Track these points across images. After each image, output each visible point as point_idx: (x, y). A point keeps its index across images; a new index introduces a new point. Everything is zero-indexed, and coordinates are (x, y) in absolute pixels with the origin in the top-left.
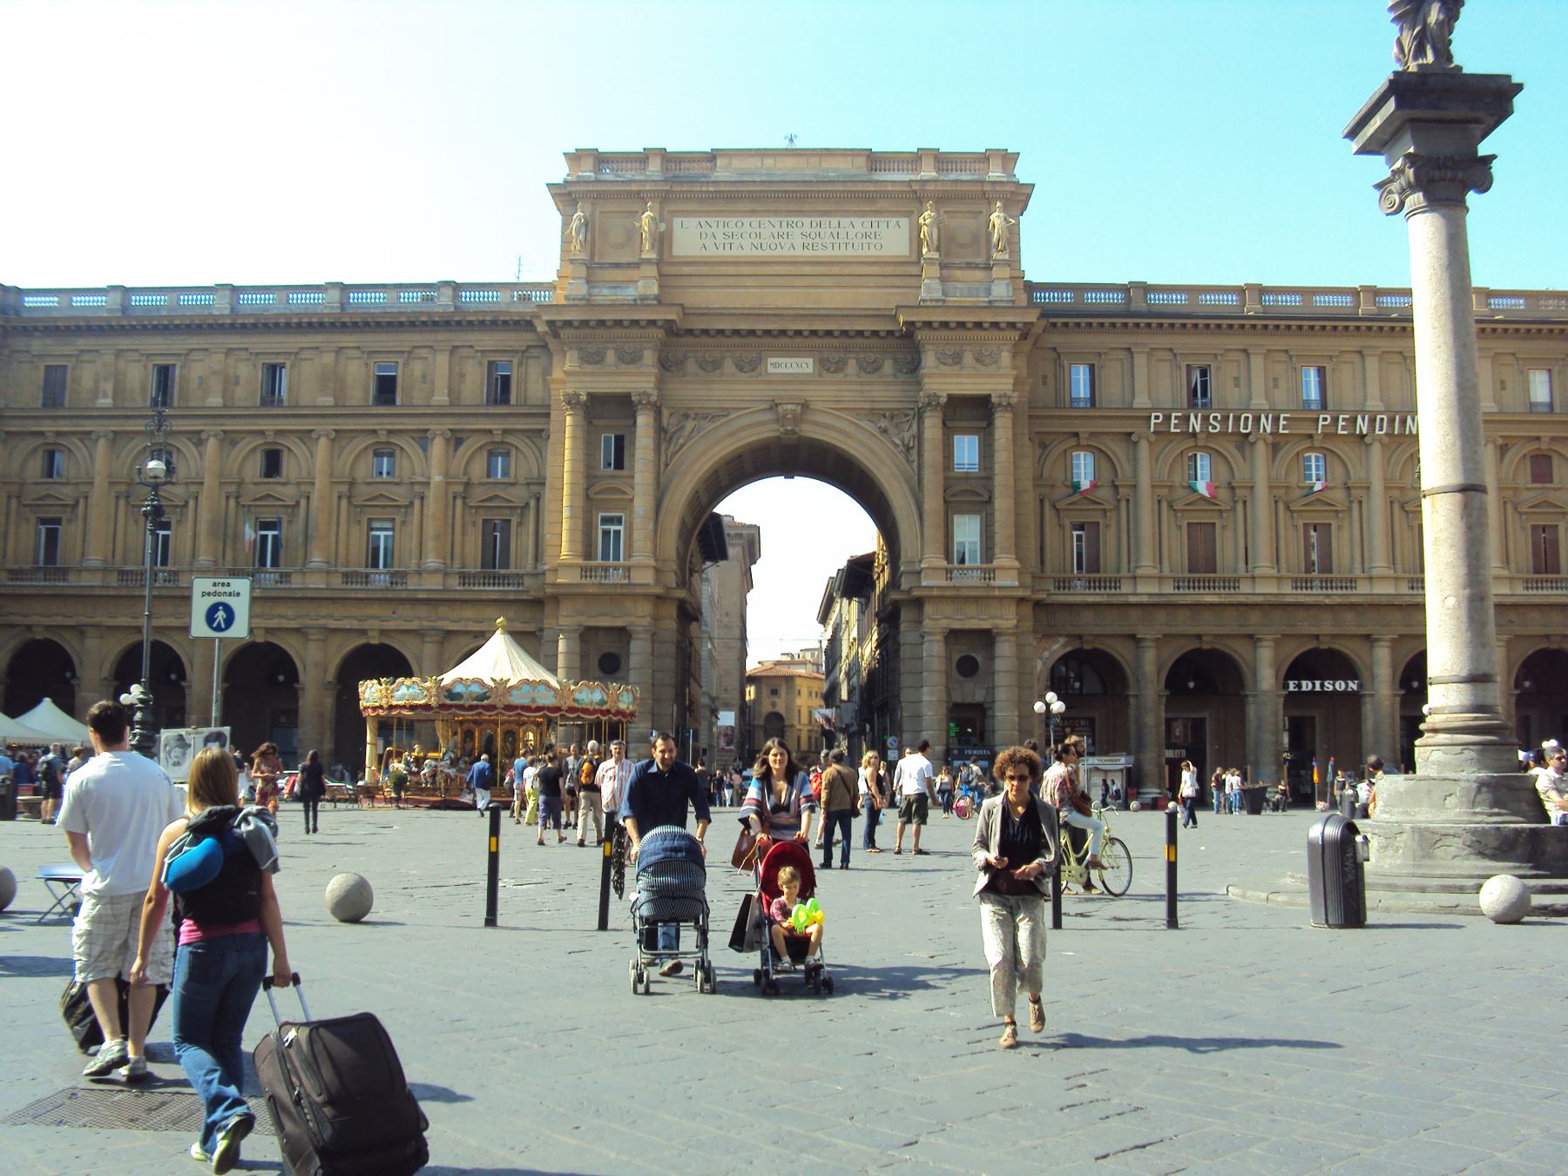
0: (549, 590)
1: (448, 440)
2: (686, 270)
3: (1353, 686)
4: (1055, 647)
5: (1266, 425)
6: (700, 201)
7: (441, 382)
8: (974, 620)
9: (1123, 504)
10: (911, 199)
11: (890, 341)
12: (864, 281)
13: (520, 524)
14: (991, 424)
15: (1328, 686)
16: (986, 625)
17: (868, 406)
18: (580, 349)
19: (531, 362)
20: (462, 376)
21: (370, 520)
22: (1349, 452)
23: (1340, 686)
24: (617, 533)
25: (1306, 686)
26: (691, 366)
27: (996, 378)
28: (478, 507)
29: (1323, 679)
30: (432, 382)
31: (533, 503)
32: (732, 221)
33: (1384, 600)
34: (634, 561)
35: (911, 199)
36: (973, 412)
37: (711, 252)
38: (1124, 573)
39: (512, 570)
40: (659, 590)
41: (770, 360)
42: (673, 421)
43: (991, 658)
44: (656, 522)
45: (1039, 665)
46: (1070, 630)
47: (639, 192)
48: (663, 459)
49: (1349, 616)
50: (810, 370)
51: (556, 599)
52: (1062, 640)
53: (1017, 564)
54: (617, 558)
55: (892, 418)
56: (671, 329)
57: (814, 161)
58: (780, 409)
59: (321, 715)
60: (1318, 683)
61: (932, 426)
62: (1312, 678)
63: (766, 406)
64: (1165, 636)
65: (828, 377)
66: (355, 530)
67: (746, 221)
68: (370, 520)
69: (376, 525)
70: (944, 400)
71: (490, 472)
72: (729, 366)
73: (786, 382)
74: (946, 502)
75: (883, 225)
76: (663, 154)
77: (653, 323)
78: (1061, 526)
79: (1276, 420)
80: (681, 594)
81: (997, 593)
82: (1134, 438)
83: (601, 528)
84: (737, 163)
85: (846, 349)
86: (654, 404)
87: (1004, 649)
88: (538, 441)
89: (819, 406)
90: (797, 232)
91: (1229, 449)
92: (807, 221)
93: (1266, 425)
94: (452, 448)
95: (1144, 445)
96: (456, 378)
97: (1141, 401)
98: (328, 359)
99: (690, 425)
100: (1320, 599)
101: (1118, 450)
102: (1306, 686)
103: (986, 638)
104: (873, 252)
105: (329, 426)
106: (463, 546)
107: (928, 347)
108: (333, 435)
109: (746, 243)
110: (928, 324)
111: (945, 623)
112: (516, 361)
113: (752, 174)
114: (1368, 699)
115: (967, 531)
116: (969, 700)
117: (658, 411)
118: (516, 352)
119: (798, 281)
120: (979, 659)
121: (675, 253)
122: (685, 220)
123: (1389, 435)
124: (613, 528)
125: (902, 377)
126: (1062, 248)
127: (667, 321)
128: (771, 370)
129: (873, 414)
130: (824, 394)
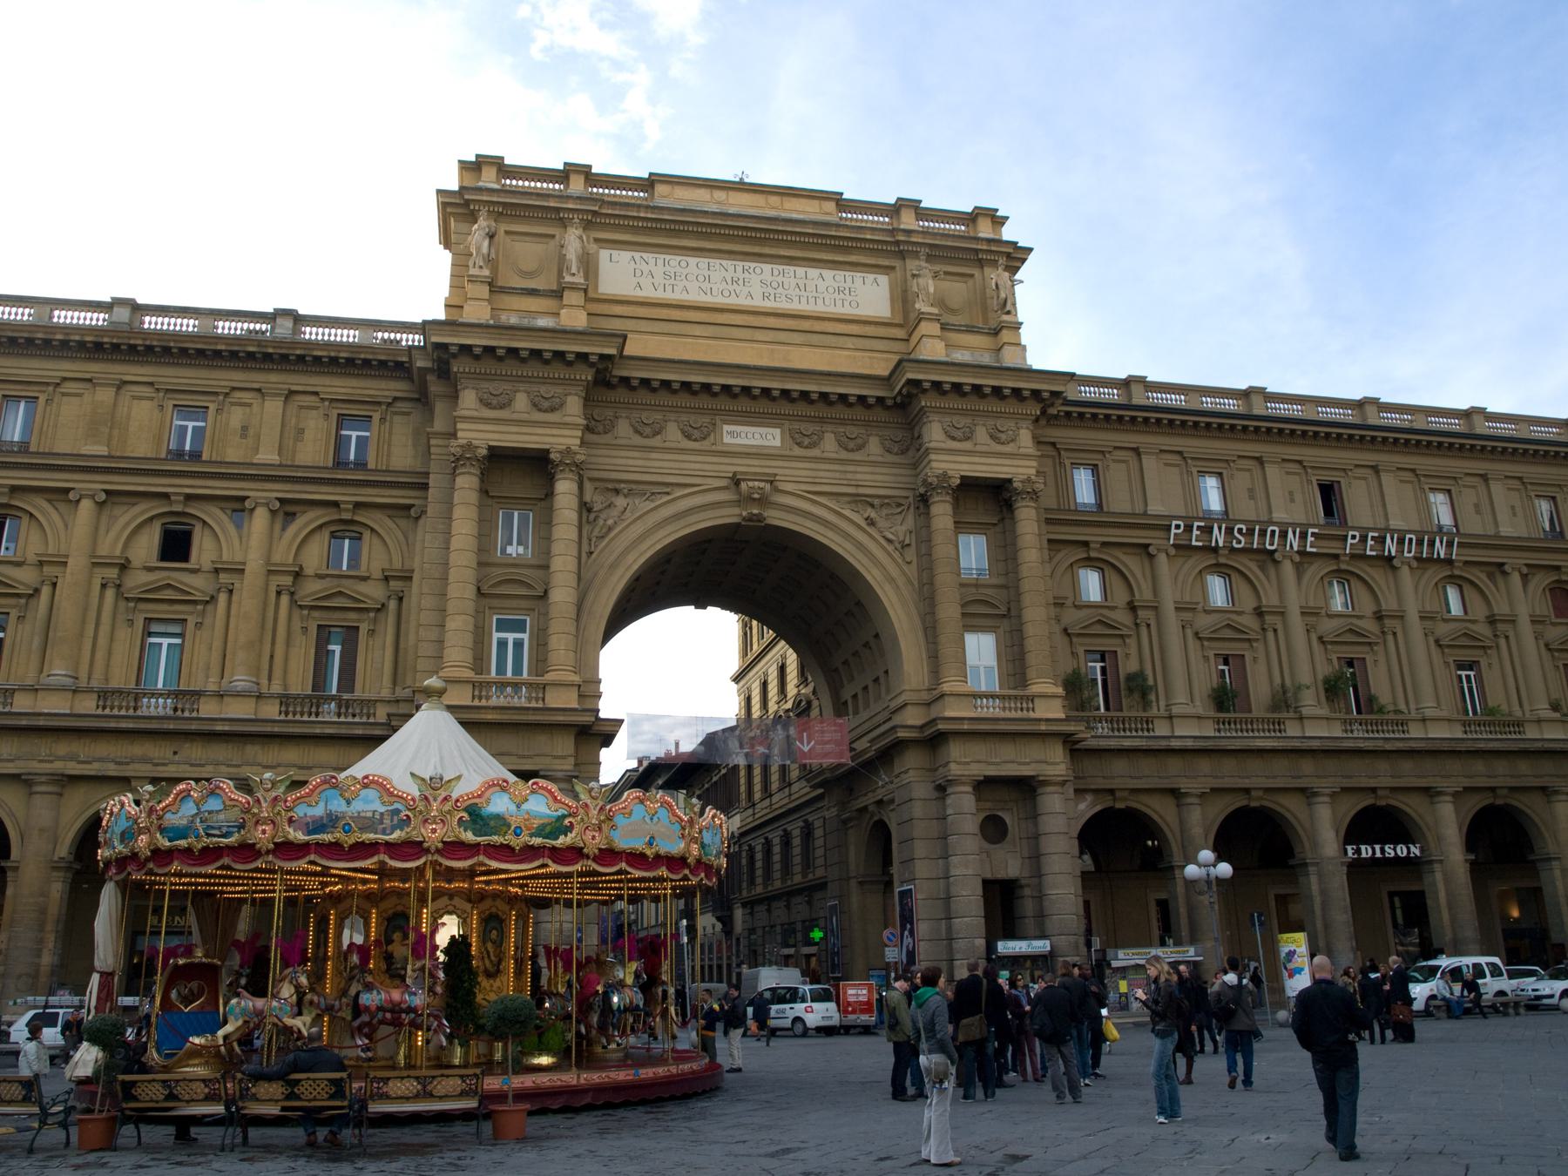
1: (273, 512)
2: (618, 310)
3: (1415, 851)
4: (1082, 806)
5: (1293, 541)
6: (636, 230)
7: (270, 436)
9: (1144, 630)
11: (880, 414)
12: (841, 341)
13: (372, 632)
15: (1390, 851)
16: (1026, 771)
19: (397, 419)
20: (301, 431)
21: (148, 620)
22: (1376, 575)
23: (1402, 851)
25: (1366, 851)
26: (623, 429)
29: (1383, 842)
30: (258, 436)
31: (393, 604)
32: (674, 260)
33: (1446, 746)
36: (989, 499)
37: (648, 293)
39: (358, 694)
41: (726, 428)
43: (1034, 816)
46: (1101, 783)
47: (558, 210)
48: (585, 548)
49: (1407, 765)
50: (777, 443)
52: (1089, 798)
57: (774, 200)
58: (743, 485)
59: (43, 911)
60: (1377, 847)
61: (942, 511)
62: (1371, 843)
63: (723, 483)
64: (1213, 790)
65: (798, 451)
66: (123, 633)
67: (693, 261)
68: (148, 620)
69: (155, 628)
71: (333, 558)
73: (748, 455)
77: (583, 357)
79: (1303, 536)
82: (1151, 550)
83: (496, 636)
85: (822, 420)
88: (403, 523)
89: (789, 487)
90: (755, 279)
91: (1250, 566)
92: (767, 267)
93: (1293, 541)
94: (278, 526)
95: (1162, 557)
96: (291, 435)
97: (1155, 508)
98: (105, 395)
99: (620, 502)
100: (1380, 743)
101: (1133, 564)
102: (1366, 851)
103: (1026, 788)
105: (97, 484)
106: (286, 660)
107: (933, 417)
108: (103, 496)
109: (693, 286)
110: (937, 385)
112: (376, 416)
114: (1437, 866)
115: (981, 650)
118: (379, 403)
119: (759, 335)
121: (601, 290)
122: (615, 253)
123: (1418, 559)
124: (511, 637)
125: (890, 458)
126: (1062, 329)
127: (603, 357)
128: (727, 439)
129: (858, 500)
130: (796, 476)
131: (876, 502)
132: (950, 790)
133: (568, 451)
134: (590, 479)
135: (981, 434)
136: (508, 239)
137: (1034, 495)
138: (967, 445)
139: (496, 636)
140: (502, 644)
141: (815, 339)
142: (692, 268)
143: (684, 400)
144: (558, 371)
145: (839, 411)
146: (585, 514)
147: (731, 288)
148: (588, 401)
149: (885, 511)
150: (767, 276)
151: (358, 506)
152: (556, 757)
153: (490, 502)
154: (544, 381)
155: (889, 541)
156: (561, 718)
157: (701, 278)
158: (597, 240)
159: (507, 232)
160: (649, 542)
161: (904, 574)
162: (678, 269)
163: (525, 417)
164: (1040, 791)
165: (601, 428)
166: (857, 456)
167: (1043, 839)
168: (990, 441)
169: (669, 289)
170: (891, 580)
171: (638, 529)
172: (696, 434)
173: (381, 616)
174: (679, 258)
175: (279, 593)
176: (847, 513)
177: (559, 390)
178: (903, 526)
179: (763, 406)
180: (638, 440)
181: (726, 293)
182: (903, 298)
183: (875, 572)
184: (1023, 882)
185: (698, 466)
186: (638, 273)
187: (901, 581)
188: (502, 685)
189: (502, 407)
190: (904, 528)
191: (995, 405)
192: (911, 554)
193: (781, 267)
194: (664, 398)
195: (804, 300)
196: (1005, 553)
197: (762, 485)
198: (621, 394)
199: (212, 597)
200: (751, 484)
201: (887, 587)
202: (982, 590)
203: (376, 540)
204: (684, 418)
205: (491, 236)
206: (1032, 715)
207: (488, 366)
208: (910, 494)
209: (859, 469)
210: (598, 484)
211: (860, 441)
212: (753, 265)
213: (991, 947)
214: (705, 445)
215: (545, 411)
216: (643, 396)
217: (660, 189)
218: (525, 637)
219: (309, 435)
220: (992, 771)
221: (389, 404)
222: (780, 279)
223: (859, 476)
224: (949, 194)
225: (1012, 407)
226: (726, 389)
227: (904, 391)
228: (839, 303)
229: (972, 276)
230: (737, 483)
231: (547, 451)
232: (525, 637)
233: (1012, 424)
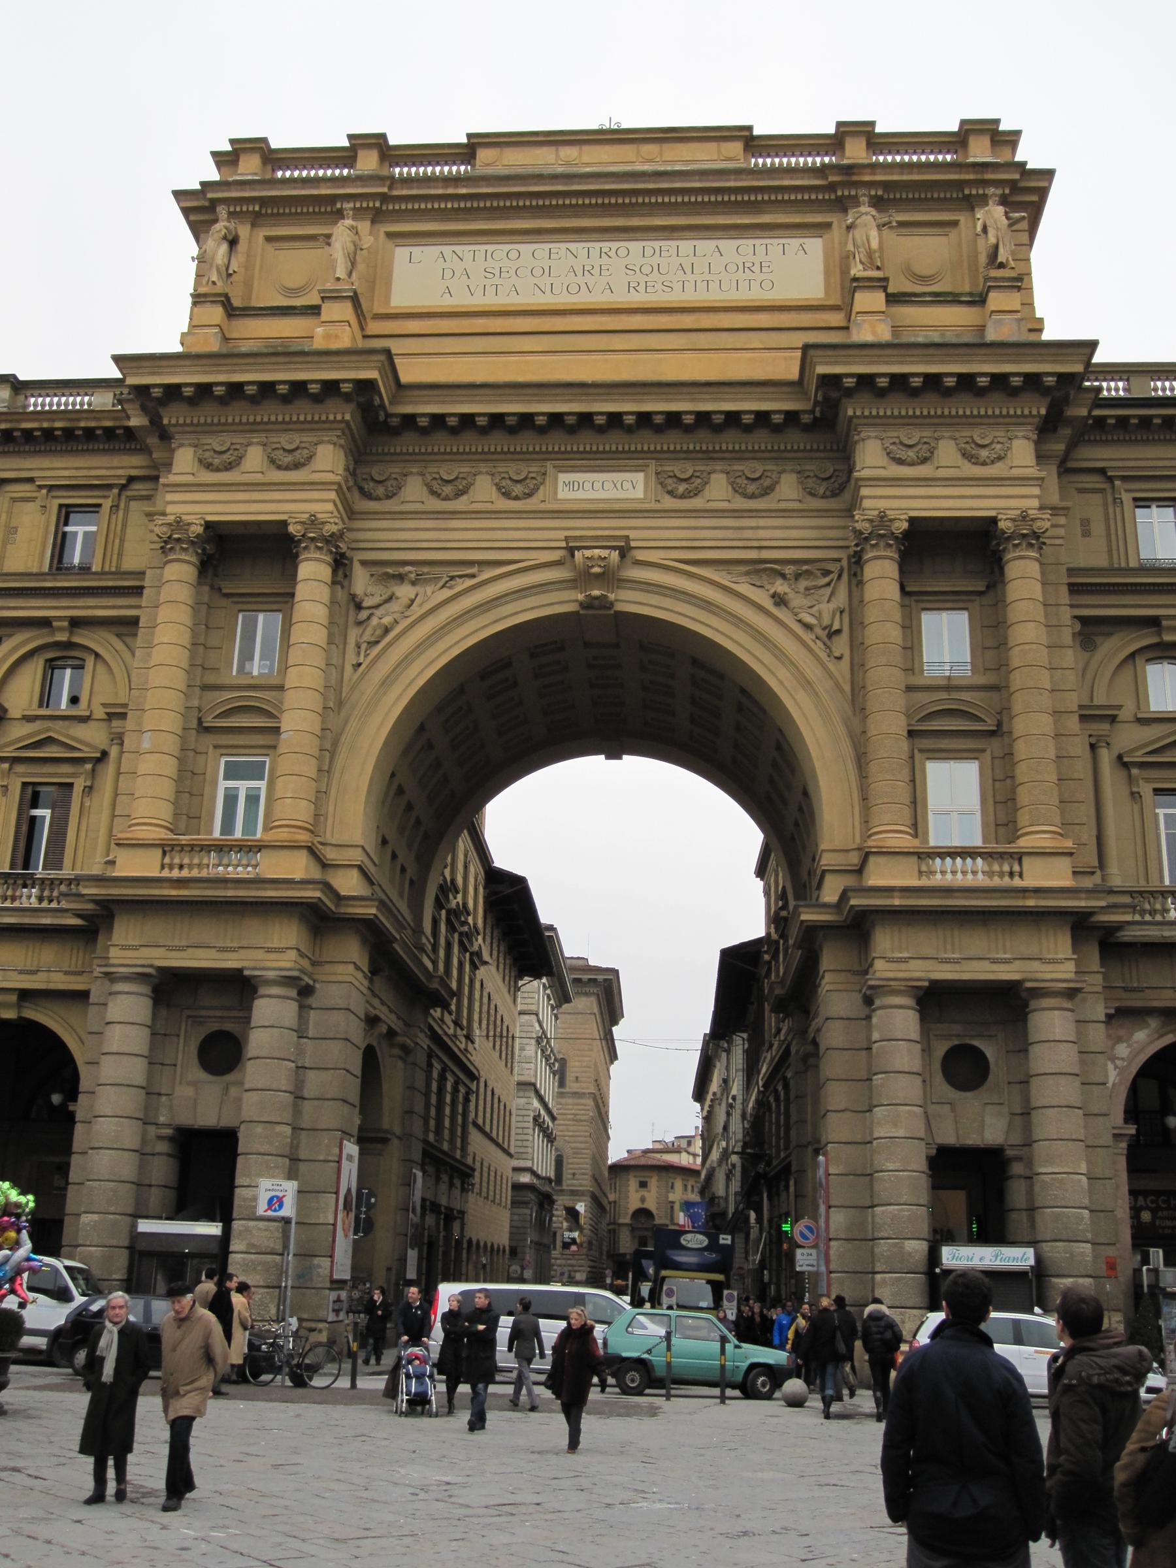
4: (1140, 1036)
11: (795, 439)
13: (88, 790)
19: (134, 505)
26: (414, 491)
28: (15, 760)
32: (500, 251)
34: (271, 836)
37: (461, 300)
41: (563, 477)
43: (1022, 1047)
45: (1112, 1076)
48: (351, 658)
50: (639, 493)
52: (1154, 1023)
61: (882, 575)
63: (555, 556)
65: (669, 503)
67: (526, 249)
71: (46, 696)
77: (331, 387)
78: (1135, 796)
83: (223, 785)
85: (708, 456)
87: (1051, 1024)
92: (635, 246)
99: (405, 591)
103: (1008, 1003)
110: (866, 381)
112: (107, 504)
116: (972, 1140)
117: (340, 564)
118: (109, 487)
119: (618, 342)
122: (416, 250)
124: (243, 787)
128: (563, 493)
129: (759, 569)
131: (789, 570)
132: (877, 1003)
134: (364, 563)
135: (947, 453)
136: (270, 248)
137: (1035, 539)
139: (223, 785)
140: (231, 799)
141: (702, 340)
143: (498, 441)
144: (302, 411)
145: (731, 440)
146: (352, 612)
147: (580, 280)
148: (361, 455)
149: (803, 584)
150: (635, 259)
151: (76, 623)
152: (270, 950)
153: (225, 602)
154: (286, 426)
155: (808, 627)
158: (390, 235)
159: (269, 239)
160: (441, 646)
161: (830, 675)
163: (259, 478)
164: (1033, 1004)
167: (1034, 1082)
168: (960, 461)
169: (490, 291)
170: (807, 684)
172: (518, 489)
173: (99, 767)
174: (507, 247)
176: (744, 589)
177: (308, 438)
178: (828, 607)
179: (614, 441)
182: (837, 266)
183: (783, 673)
184: (1010, 1153)
186: (448, 274)
187: (823, 686)
188: (221, 848)
189: (229, 467)
190: (832, 606)
191: (964, 406)
192: (841, 645)
193: (656, 244)
194: (469, 442)
195: (689, 286)
196: (992, 638)
197: (604, 553)
198: (408, 442)
200: (588, 553)
201: (801, 696)
202: (955, 695)
203: (101, 669)
205: (233, 242)
206: (1017, 882)
208: (843, 555)
209: (762, 522)
210: (374, 570)
211: (767, 483)
212: (614, 245)
213: (934, 1257)
214: (531, 504)
215: (287, 468)
216: (440, 442)
217: (483, 155)
218: (262, 785)
219: (22, 534)
221: (123, 487)
222: (656, 260)
223: (762, 534)
224: (918, 103)
225: (996, 405)
226: (556, 419)
227: (820, 398)
228: (743, 285)
229: (955, 224)
230: (571, 551)
231: (285, 523)
232: (262, 785)
233: (1000, 433)
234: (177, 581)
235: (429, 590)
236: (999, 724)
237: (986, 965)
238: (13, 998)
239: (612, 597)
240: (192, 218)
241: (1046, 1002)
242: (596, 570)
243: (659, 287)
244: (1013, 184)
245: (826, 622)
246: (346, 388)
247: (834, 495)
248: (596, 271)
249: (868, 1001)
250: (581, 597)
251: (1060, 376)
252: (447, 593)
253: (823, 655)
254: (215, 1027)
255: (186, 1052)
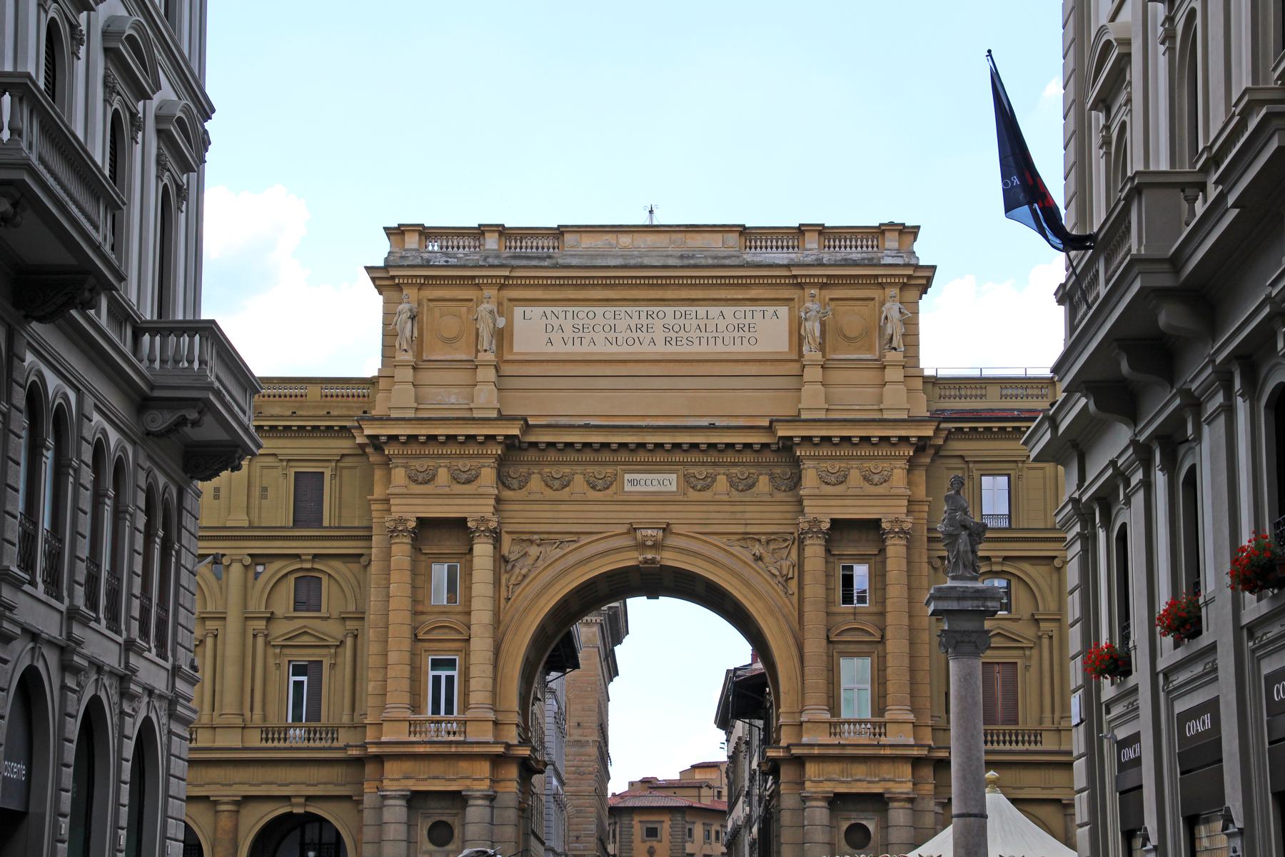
0: (372, 750)
8: (861, 781)
9: (1045, 641)
10: (794, 281)
11: (768, 457)
13: (333, 666)
14: (882, 551)
16: (877, 789)
17: (741, 529)
18: (406, 467)
19: (345, 472)
20: (264, 489)
24: (450, 679)
26: (535, 483)
27: (886, 493)
31: (349, 641)
32: (582, 310)
35: (794, 281)
37: (559, 349)
38: (1047, 724)
40: (500, 749)
41: (627, 477)
42: (517, 548)
43: (885, 826)
44: (495, 666)
47: (474, 277)
48: (504, 594)
51: (379, 759)
53: (911, 717)
54: (449, 710)
55: (768, 542)
56: (511, 444)
61: (814, 551)
63: (624, 529)
65: (693, 495)
67: (599, 311)
70: (826, 526)
72: (579, 483)
74: (829, 641)
75: (758, 315)
76: (502, 231)
80: (525, 752)
81: (888, 752)
84: (587, 241)
85: (715, 464)
86: (494, 531)
90: (658, 324)
92: (669, 310)
99: (534, 551)
104: (746, 348)
111: (830, 788)
113: (603, 256)
115: (855, 674)
117: (496, 537)
120: (871, 826)
122: (528, 310)
124: (443, 674)
125: (780, 496)
127: (507, 437)
128: (628, 488)
129: (746, 537)
131: (763, 538)
133: (483, 520)
134: (508, 533)
138: (839, 489)
139: (431, 673)
140: (437, 680)
142: (600, 320)
143: (588, 456)
145: (729, 457)
147: (635, 335)
149: (772, 546)
153: (423, 558)
156: (477, 749)
157: (607, 328)
160: (558, 587)
162: (586, 321)
163: (447, 490)
165: (516, 486)
166: (746, 497)
169: (577, 341)
171: (547, 576)
173: (340, 650)
175: (255, 636)
176: (736, 550)
179: (659, 457)
180: (549, 494)
181: (630, 342)
185: (602, 515)
193: (683, 309)
195: (704, 341)
197: (654, 533)
198: (532, 455)
199: (201, 641)
200: (644, 532)
203: (332, 582)
204: (590, 469)
207: (413, 449)
210: (515, 536)
211: (750, 481)
212: (656, 309)
216: (552, 456)
218: (455, 673)
220: (842, 789)
221: (338, 461)
222: (682, 322)
223: (747, 515)
226: (623, 446)
228: (738, 341)
229: (873, 299)
234: (401, 551)
235: (548, 549)
236: (883, 637)
237: (865, 784)
238: (302, 800)
239: (658, 558)
240: (378, 282)
241: (896, 804)
242: (649, 543)
243: (684, 341)
244: (909, 277)
245: (785, 572)
246: (500, 439)
247: (791, 490)
248: (644, 329)
249: (804, 802)
250: (641, 558)
251: (919, 438)
252: (559, 552)
253: (782, 594)
254: (437, 819)
255: (422, 832)
